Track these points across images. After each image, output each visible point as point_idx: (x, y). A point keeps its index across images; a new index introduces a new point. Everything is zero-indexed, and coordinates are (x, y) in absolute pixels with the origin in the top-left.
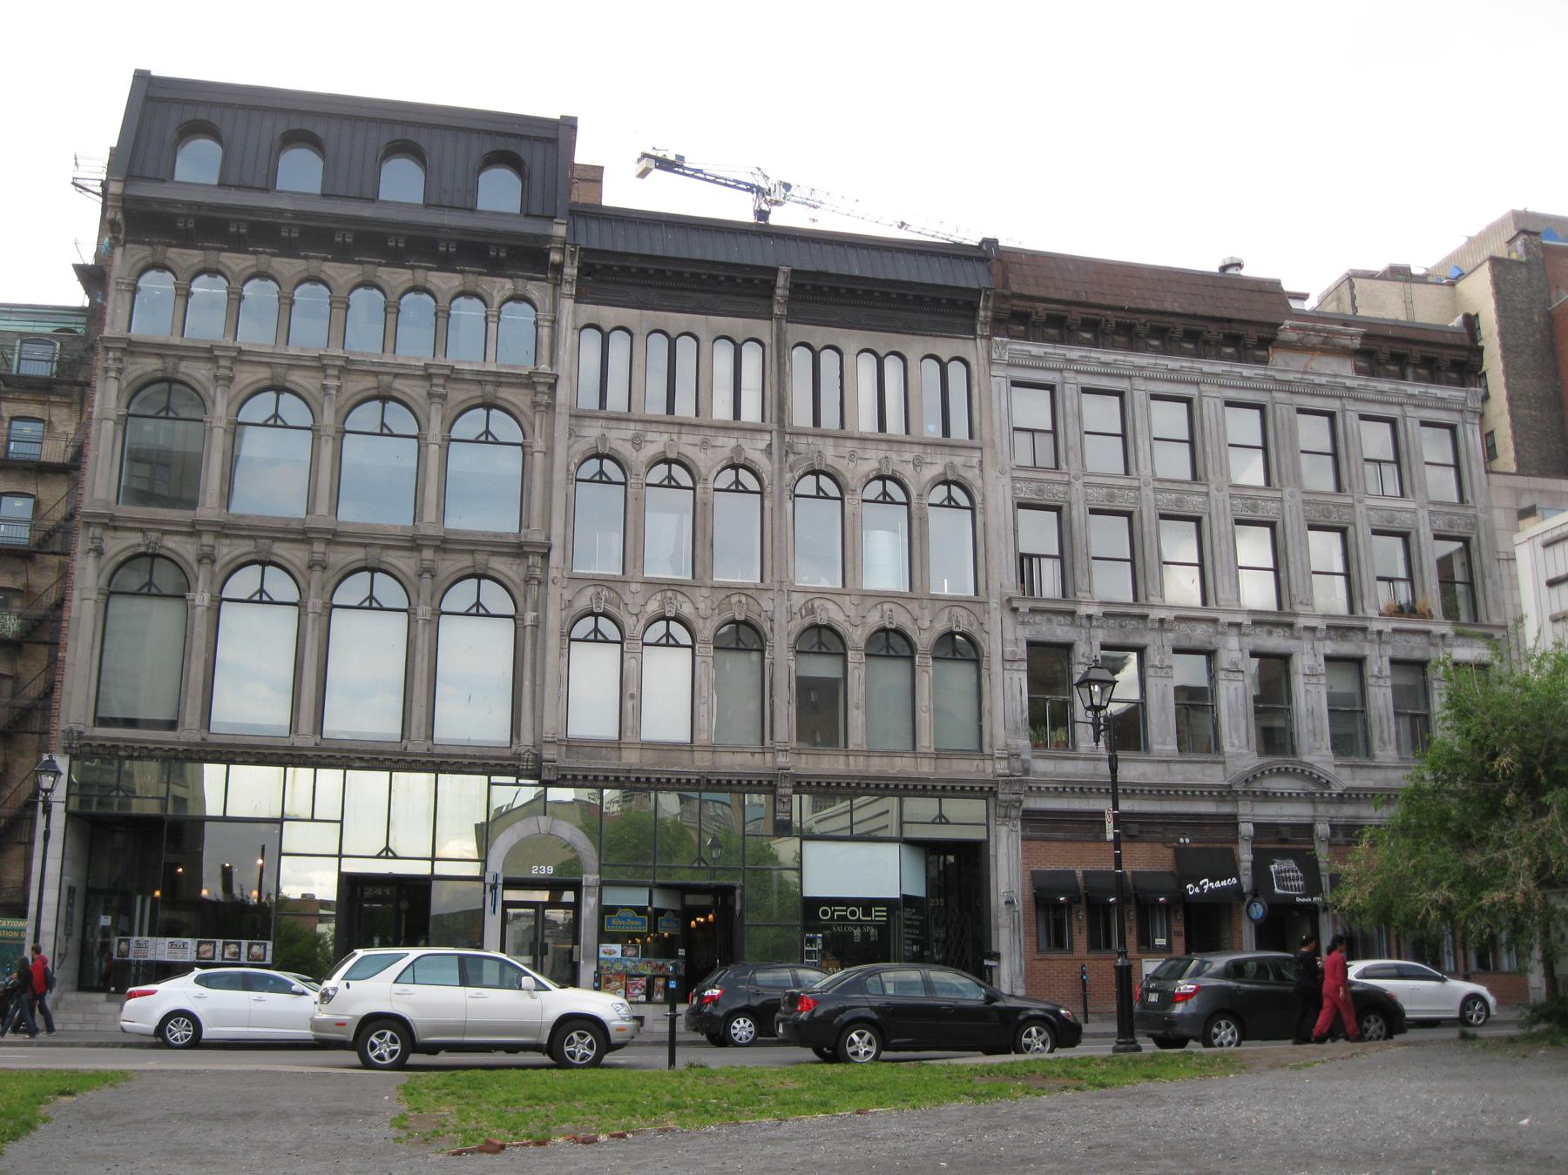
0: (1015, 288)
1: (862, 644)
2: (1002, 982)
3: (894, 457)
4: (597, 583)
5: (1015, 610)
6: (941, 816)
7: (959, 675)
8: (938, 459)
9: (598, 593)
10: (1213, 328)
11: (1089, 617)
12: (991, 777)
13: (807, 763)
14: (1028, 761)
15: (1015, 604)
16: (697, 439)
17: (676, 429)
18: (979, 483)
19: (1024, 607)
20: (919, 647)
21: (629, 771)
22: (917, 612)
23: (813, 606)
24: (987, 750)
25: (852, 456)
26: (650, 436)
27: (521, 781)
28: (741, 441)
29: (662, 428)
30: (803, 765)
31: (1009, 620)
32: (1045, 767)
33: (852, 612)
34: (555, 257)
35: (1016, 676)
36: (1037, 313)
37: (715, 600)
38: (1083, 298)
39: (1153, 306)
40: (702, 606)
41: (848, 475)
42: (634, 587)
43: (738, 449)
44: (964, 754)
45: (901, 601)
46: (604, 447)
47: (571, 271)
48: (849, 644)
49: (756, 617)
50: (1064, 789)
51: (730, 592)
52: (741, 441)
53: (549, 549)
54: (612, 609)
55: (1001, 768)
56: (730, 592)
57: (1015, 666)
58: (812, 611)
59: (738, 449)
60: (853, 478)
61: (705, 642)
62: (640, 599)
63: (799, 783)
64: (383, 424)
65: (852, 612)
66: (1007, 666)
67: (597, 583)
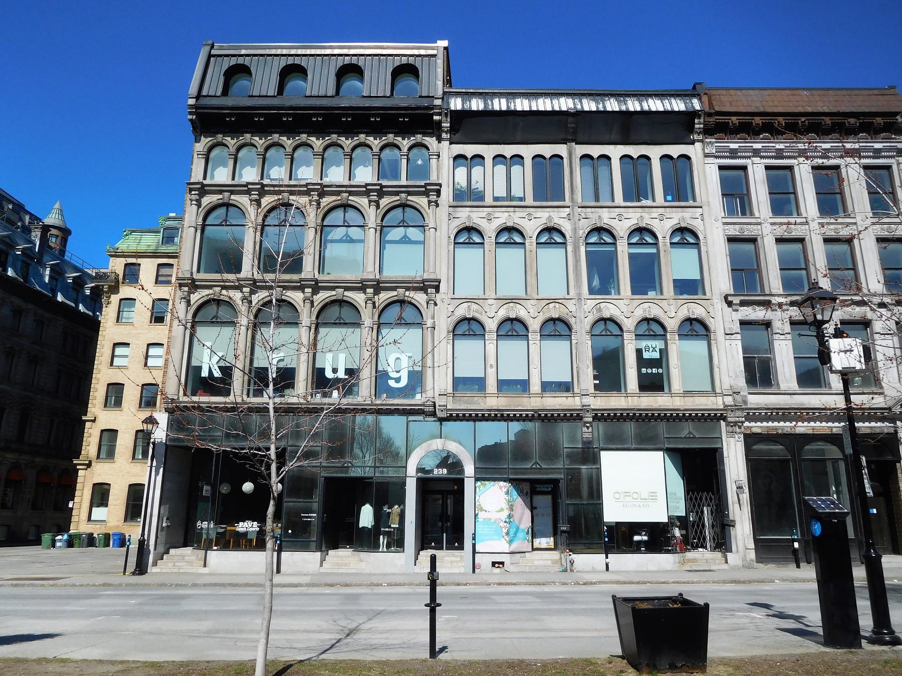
1: (632, 329)
2: (738, 540)
3: (646, 215)
4: (469, 300)
5: (730, 304)
7: (698, 347)
8: (674, 215)
9: (469, 306)
10: (852, 121)
11: (780, 305)
12: (722, 407)
14: (746, 396)
15: (730, 299)
16: (524, 215)
17: (512, 209)
18: (702, 228)
19: (736, 300)
20: (669, 329)
21: (490, 410)
22: (666, 308)
23: (600, 307)
24: (718, 391)
25: (620, 217)
26: (497, 215)
27: (426, 419)
28: (551, 214)
29: (504, 209)
32: (757, 400)
33: (624, 309)
34: (436, 118)
36: (732, 122)
37: (539, 307)
38: (762, 110)
39: (809, 110)
40: (531, 311)
41: (618, 229)
42: (490, 302)
43: (550, 218)
44: (701, 393)
45: (655, 301)
46: (470, 222)
47: (446, 125)
48: (625, 329)
49: (567, 317)
51: (548, 302)
52: (551, 214)
54: (477, 316)
55: (729, 400)
56: (548, 302)
57: (733, 337)
58: (600, 310)
59: (550, 218)
61: (534, 332)
62: (494, 308)
63: (596, 414)
64: (345, 221)
65: (624, 309)
66: (728, 337)
67: (469, 300)
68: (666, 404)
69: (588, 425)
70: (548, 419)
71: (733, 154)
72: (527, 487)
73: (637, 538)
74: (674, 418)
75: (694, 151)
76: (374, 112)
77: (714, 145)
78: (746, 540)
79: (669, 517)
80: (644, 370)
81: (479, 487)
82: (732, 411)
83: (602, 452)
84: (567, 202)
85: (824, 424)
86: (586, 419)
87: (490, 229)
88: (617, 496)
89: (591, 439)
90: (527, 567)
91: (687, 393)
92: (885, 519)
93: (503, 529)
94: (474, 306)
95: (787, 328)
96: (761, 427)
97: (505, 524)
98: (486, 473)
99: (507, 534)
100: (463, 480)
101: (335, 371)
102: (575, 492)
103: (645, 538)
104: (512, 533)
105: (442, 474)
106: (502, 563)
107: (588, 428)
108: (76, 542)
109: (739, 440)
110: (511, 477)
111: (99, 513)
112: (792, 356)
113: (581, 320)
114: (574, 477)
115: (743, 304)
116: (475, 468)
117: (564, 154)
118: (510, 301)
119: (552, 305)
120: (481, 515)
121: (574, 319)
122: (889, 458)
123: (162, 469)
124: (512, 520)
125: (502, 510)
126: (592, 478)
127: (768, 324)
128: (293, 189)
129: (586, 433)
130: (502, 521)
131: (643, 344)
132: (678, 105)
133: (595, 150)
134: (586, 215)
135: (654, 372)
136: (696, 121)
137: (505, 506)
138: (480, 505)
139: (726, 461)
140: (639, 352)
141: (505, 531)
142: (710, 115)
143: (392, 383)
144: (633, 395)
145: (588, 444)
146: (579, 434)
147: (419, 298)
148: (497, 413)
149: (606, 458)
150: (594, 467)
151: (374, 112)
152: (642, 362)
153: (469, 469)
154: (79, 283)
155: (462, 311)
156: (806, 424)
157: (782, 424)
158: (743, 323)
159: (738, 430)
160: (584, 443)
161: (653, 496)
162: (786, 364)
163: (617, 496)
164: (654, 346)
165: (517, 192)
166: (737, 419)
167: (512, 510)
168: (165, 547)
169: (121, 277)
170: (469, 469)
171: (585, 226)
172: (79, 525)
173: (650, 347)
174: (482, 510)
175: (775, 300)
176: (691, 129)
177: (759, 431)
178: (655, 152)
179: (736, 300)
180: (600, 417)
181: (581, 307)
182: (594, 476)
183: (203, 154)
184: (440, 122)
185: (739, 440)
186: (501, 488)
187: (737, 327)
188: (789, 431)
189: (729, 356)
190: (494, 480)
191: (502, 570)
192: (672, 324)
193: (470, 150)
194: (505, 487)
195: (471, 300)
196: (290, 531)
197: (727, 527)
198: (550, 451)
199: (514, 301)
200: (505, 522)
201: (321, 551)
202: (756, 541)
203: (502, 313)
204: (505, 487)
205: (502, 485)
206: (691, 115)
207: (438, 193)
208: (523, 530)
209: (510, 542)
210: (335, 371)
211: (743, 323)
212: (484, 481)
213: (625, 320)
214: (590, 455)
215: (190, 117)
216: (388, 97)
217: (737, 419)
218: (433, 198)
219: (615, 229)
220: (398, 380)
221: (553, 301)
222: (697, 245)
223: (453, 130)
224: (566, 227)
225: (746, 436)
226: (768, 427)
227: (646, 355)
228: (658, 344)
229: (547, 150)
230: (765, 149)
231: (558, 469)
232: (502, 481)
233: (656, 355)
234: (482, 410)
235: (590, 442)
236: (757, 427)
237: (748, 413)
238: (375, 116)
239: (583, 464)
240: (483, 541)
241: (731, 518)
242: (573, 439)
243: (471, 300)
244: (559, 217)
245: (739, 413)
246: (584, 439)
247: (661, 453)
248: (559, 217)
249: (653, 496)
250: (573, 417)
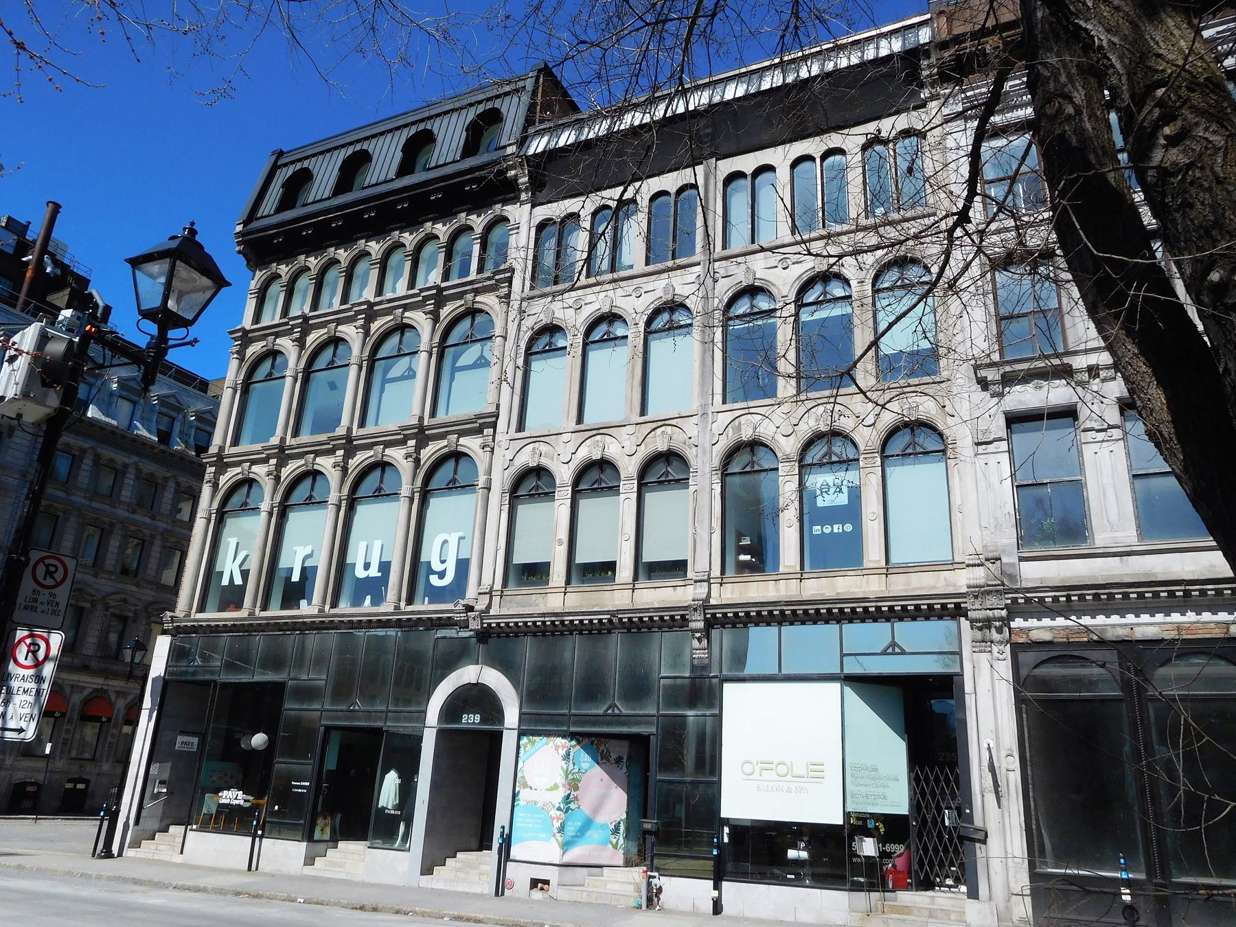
5: (984, 384)
6: (893, 644)
13: (732, 593)
14: (1012, 565)
15: (983, 373)
21: (544, 615)
30: (729, 596)
31: (979, 395)
34: (512, 173)
35: (992, 460)
37: (640, 436)
40: (626, 444)
42: (566, 437)
50: (1068, 597)
51: (654, 425)
53: (497, 418)
56: (654, 425)
57: (991, 448)
60: (784, 284)
68: (851, 590)
69: (698, 635)
72: (619, 749)
73: (792, 854)
76: (434, 187)
78: (1011, 873)
79: (847, 815)
80: (848, 528)
81: (525, 746)
82: (976, 597)
83: (726, 686)
85: (1206, 616)
86: (693, 625)
88: (748, 768)
89: (707, 661)
90: (585, 894)
92: (312, 797)
93: (555, 821)
96: (1052, 628)
97: (559, 813)
98: (537, 722)
99: (562, 829)
100: (502, 732)
101: (367, 566)
103: (804, 855)
104: (571, 829)
105: (474, 723)
106: (547, 882)
107: (699, 640)
109: (1001, 657)
110: (572, 729)
113: (704, 449)
114: (674, 730)
116: (521, 714)
118: (595, 432)
119: (659, 431)
120: (524, 795)
121: (694, 449)
123: (156, 712)
124: (572, 806)
125: (555, 787)
126: (705, 733)
127: (1068, 414)
128: (339, 316)
129: (697, 649)
130: (554, 806)
134: (727, 271)
135: (836, 530)
136: (924, 63)
137: (560, 780)
138: (523, 777)
139: (969, 701)
141: (557, 824)
143: (434, 580)
144: (787, 577)
145: (700, 671)
146: (688, 651)
147: (471, 444)
148: (553, 619)
150: (708, 713)
151: (434, 187)
152: (808, 513)
153: (511, 716)
156: (1159, 617)
157: (1101, 620)
158: (1015, 420)
159: (995, 636)
160: (694, 668)
161: (816, 771)
162: (1110, 493)
163: (748, 768)
164: (838, 482)
166: (990, 613)
167: (576, 788)
168: (161, 821)
170: (511, 716)
173: (831, 484)
174: (525, 785)
175: (1079, 362)
177: (1047, 636)
181: (706, 426)
182: (709, 729)
183: (255, 293)
184: (516, 178)
185: (1001, 657)
186: (557, 748)
187: (998, 427)
188: (1122, 633)
189: (982, 484)
190: (548, 734)
191: (546, 895)
194: (563, 747)
195: (538, 439)
196: (276, 808)
197: (968, 843)
198: (638, 687)
199: (601, 431)
200: (559, 809)
201: (309, 838)
202: (1034, 876)
204: (563, 747)
205: (559, 744)
206: (912, 56)
208: (603, 827)
209: (566, 846)
210: (367, 566)
212: (533, 735)
213: (782, 440)
215: (237, 249)
216: (458, 161)
217: (990, 613)
219: (773, 285)
220: (442, 575)
221: (663, 423)
225: (1017, 649)
226: (1067, 628)
229: (670, 182)
232: (559, 736)
233: (843, 499)
234: (531, 615)
235: (705, 668)
236: (1041, 628)
237: (1015, 600)
238: (436, 191)
239: (692, 705)
240: (521, 840)
241: (978, 822)
242: (676, 662)
243: (538, 439)
244: (683, 284)
245: (992, 601)
246: (696, 662)
247: (836, 686)
249: (816, 771)
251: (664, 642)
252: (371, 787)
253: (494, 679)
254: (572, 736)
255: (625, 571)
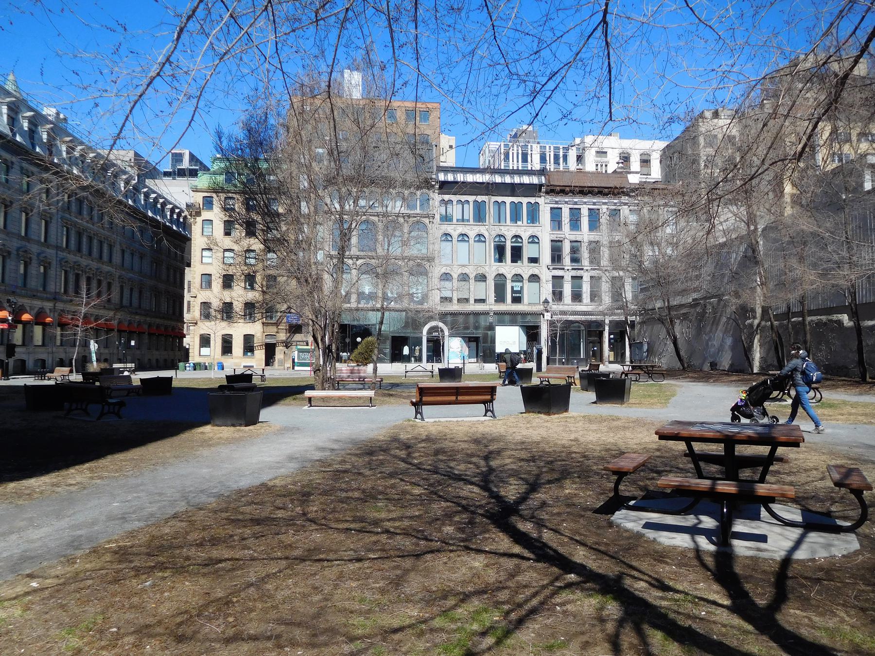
0: (552, 183)
3: (519, 230)
5: (549, 269)
10: (606, 190)
33: (508, 270)
43: (480, 231)
44: (535, 304)
65: (508, 270)
70: (477, 314)
71: (557, 203)
72: (467, 339)
74: (524, 314)
75: (541, 200)
77: (549, 198)
84: (487, 223)
87: (455, 235)
91: (529, 304)
94: (448, 268)
95: (570, 279)
102: (485, 341)
108: (197, 367)
111: (205, 351)
112: (570, 290)
114: (486, 336)
115: (554, 269)
117: (487, 201)
120: (451, 350)
122: (601, 329)
127: (563, 277)
129: (491, 319)
131: (514, 284)
132: (535, 180)
133: (500, 199)
140: (512, 287)
142: (548, 186)
144: (509, 305)
149: (499, 329)
152: (513, 291)
153: (446, 333)
154: (156, 200)
155: (443, 270)
158: (554, 277)
165: (466, 217)
169: (201, 207)
170: (446, 333)
171: (494, 234)
172: (194, 357)
175: (566, 268)
176: (540, 190)
178: (525, 200)
179: (551, 268)
180: (496, 313)
192: (526, 277)
193: (447, 197)
203: (460, 271)
206: (541, 186)
207: (433, 218)
211: (554, 277)
214: (491, 328)
218: (431, 220)
220: (417, 298)
222: (538, 243)
223: (440, 188)
224: (486, 234)
227: (515, 289)
228: (520, 284)
229: (480, 198)
230: (570, 201)
231: (479, 333)
244: (483, 230)
248: (483, 230)
250: (486, 313)
251: (482, 318)
252: (401, 350)
253: (441, 325)
254: (462, 337)
255: (472, 301)
